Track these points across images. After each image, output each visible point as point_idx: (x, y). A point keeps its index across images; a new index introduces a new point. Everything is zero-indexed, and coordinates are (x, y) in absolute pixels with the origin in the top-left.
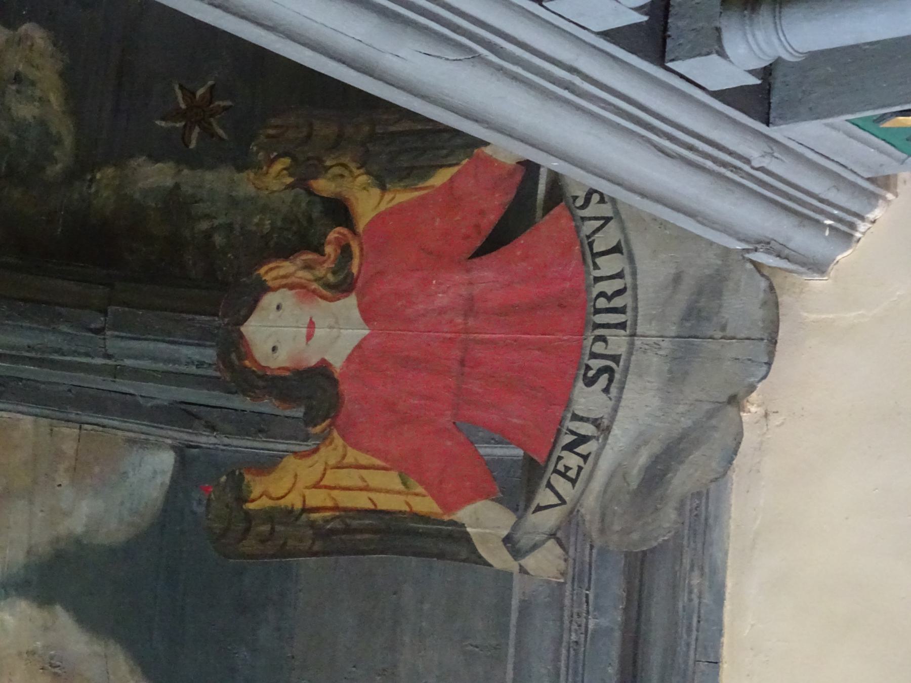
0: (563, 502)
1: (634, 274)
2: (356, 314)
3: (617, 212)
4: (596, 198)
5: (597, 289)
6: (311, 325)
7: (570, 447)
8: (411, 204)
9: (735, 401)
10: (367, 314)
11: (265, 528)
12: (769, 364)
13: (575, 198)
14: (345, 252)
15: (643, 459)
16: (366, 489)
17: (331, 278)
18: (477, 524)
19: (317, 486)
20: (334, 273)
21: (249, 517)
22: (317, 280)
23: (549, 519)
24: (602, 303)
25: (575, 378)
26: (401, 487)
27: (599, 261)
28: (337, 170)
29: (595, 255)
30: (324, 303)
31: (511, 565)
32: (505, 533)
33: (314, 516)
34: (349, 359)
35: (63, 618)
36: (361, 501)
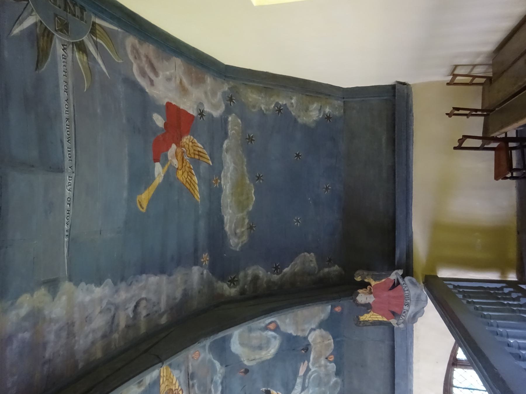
0: (403, 319)
1: (410, 293)
2: (373, 297)
3: (407, 286)
4: (404, 284)
5: (406, 295)
6: (367, 298)
7: (404, 313)
8: (379, 283)
9: (423, 308)
10: (375, 297)
11: (363, 323)
12: (427, 304)
13: (402, 284)
14: (370, 289)
15: (413, 314)
16: (377, 318)
17: (369, 292)
18: (392, 322)
19: (370, 317)
20: (369, 291)
21: (360, 322)
22: (367, 292)
23: (402, 321)
24: (406, 296)
25: (403, 305)
26: (381, 317)
27: (406, 291)
28: (368, 278)
29: (405, 291)
30: (368, 295)
31: (398, 326)
32: (396, 323)
33: (370, 321)
34: (373, 302)
35: (322, 330)
36: (376, 319)
